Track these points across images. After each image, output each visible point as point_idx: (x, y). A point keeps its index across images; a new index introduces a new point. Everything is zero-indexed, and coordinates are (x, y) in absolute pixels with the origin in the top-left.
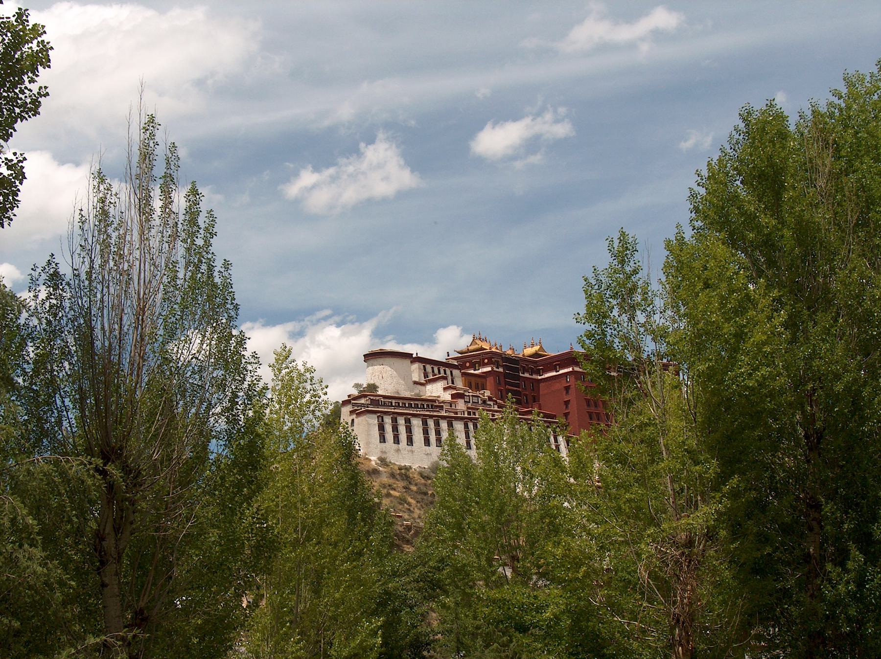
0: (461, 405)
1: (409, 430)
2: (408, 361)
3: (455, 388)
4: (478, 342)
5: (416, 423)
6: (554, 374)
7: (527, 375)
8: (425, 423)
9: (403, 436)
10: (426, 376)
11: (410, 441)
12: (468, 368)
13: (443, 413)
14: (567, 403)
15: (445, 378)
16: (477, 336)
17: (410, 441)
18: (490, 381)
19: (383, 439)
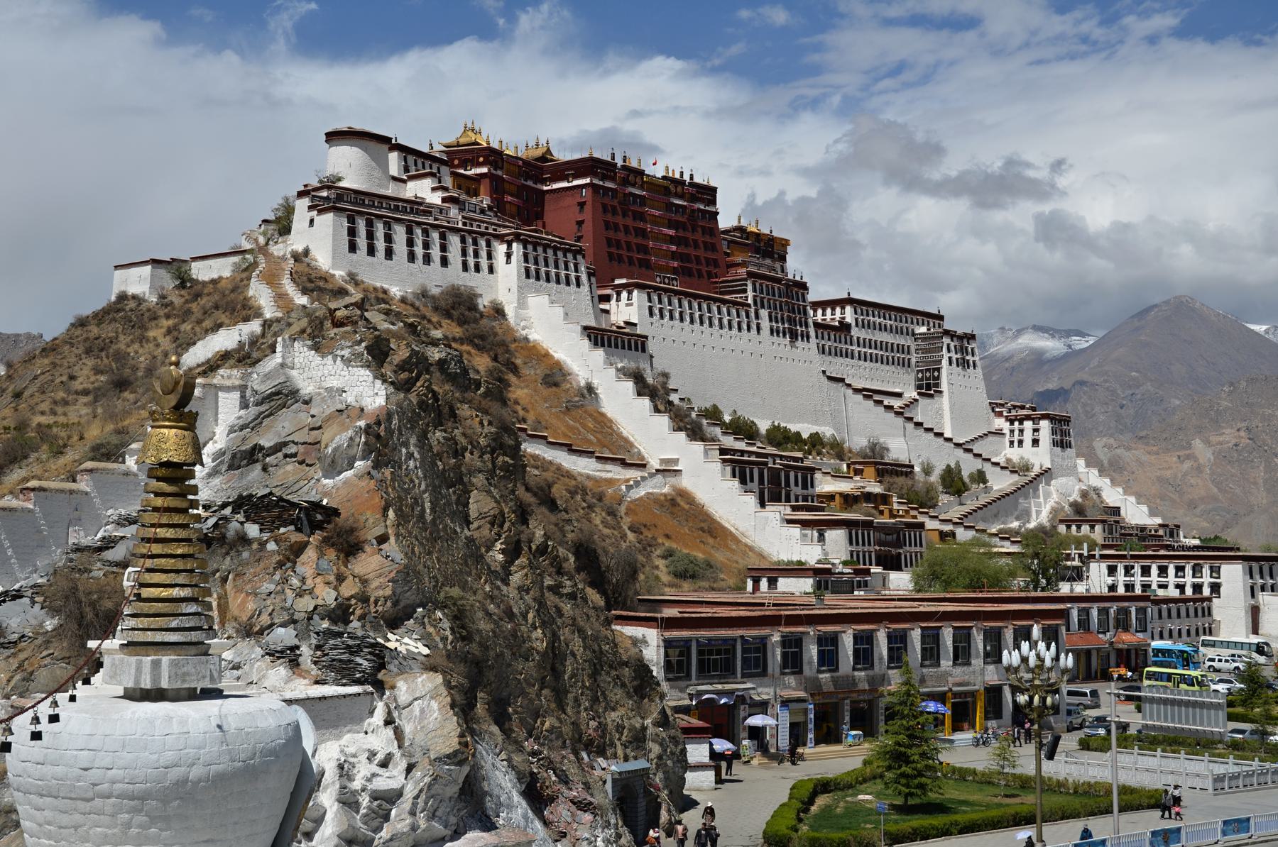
0: (454, 212)
1: (388, 238)
2: (386, 147)
3: (445, 189)
4: (470, 133)
5: (400, 233)
6: (565, 184)
7: (530, 183)
8: (410, 231)
9: (380, 245)
10: (406, 169)
11: (389, 253)
12: (458, 166)
13: (431, 220)
14: (580, 223)
15: (432, 175)
16: (469, 125)
17: (389, 253)
18: (484, 187)
19: (353, 248)
